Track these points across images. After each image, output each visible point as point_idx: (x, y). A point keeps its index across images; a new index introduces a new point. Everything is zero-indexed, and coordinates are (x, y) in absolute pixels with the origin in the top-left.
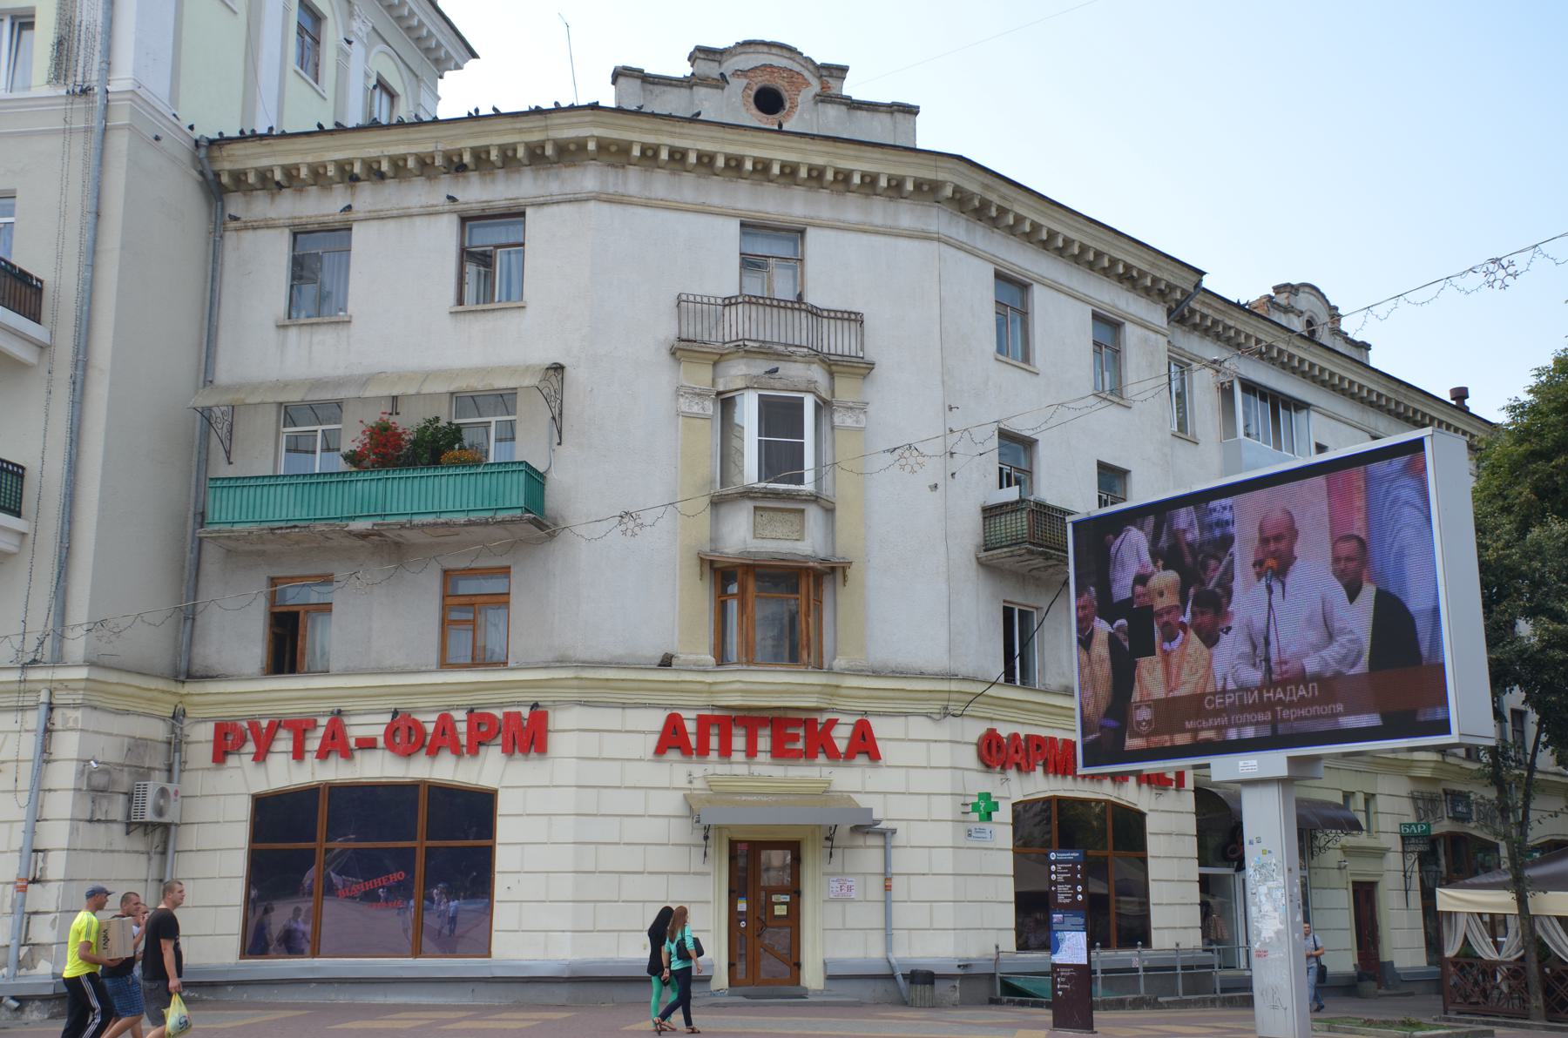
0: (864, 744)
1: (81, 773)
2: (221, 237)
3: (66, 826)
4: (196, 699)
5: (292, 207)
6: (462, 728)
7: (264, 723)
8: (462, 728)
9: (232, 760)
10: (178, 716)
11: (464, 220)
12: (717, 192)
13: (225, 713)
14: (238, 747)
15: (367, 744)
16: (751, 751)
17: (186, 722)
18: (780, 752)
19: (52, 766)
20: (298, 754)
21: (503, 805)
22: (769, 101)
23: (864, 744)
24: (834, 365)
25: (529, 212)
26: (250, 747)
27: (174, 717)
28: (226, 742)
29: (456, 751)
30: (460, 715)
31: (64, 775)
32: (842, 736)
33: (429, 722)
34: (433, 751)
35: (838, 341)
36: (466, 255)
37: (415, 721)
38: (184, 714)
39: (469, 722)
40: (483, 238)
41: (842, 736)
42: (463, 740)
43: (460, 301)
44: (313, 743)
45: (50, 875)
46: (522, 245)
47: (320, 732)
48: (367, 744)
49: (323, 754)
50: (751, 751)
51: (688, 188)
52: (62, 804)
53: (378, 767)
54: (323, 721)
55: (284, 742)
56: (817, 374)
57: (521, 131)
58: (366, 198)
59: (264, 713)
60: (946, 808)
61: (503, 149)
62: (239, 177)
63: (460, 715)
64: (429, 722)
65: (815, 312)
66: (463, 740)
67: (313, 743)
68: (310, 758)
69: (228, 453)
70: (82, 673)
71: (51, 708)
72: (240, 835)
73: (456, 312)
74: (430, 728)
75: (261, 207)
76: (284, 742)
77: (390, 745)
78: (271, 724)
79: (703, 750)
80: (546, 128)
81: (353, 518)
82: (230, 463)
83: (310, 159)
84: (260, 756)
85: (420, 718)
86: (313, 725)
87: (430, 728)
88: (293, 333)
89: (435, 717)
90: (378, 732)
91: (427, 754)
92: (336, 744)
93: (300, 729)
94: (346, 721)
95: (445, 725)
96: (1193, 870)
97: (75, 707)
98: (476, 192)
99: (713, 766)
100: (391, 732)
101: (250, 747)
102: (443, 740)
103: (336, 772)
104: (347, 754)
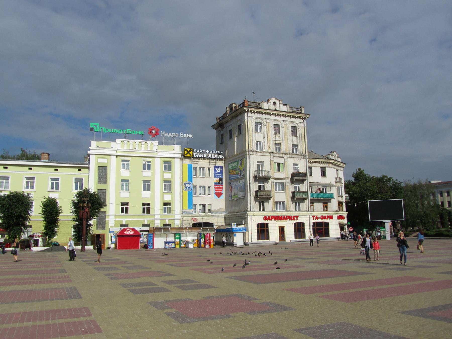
21: (330, 224)
33: (324, 216)
49: (316, 219)
53: (320, 220)
54: (315, 216)
68: (315, 219)
86: (315, 216)
90: (320, 217)
100: (321, 217)
104: (318, 219)
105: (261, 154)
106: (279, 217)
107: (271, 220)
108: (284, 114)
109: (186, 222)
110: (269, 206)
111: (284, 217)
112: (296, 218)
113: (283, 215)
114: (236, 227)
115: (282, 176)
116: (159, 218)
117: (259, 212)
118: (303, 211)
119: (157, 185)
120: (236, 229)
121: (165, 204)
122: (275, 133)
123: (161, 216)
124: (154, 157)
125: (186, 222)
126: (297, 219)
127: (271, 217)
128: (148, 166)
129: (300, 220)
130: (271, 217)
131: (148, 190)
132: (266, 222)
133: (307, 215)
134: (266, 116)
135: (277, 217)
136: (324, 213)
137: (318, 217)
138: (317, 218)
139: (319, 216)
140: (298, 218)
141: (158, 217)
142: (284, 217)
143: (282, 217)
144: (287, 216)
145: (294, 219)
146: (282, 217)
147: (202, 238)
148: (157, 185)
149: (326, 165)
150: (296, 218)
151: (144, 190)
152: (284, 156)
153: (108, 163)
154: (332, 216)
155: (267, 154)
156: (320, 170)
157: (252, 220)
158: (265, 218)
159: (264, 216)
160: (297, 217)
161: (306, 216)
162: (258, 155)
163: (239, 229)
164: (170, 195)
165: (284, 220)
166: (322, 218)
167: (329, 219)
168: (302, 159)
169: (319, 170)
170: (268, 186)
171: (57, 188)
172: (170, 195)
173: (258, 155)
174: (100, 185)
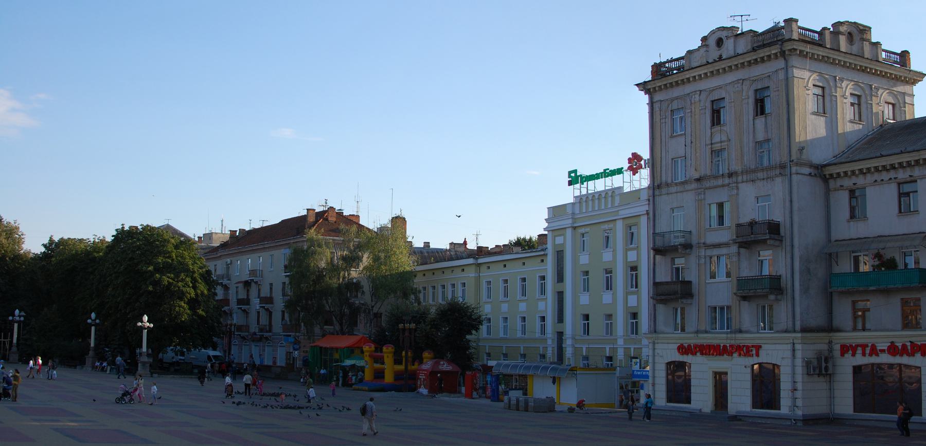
1: (803, 362)
2: (829, 194)
3: (801, 376)
4: (834, 338)
5: (848, 183)
6: (909, 348)
7: (854, 345)
8: (909, 348)
9: (846, 355)
10: (830, 342)
11: (899, 184)
14: (847, 351)
17: (833, 344)
19: (796, 360)
20: (864, 354)
25: (918, 181)
26: (850, 352)
27: (829, 343)
28: (844, 349)
29: (908, 355)
30: (908, 344)
31: (799, 362)
33: (899, 345)
34: (901, 355)
36: (901, 195)
37: (896, 346)
38: (832, 342)
39: (911, 346)
40: (906, 188)
42: (910, 351)
43: (900, 212)
44: (868, 351)
45: (798, 389)
46: (917, 191)
47: (869, 348)
49: (870, 355)
52: (799, 370)
53: (885, 358)
54: (870, 345)
55: (859, 350)
57: (911, 157)
58: (870, 178)
59: (854, 342)
61: (908, 162)
62: (831, 175)
63: (908, 344)
64: (899, 345)
66: (910, 351)
67: (868, 351)
69: (837, 262)
70: (799, 335)
71: (794, 344)
72: (850, 377)
73: (899, 216)
74: (900, 347)
75: (839, 182)
76: (859, 350)
77: (889, 353)
78: (855, 345)
80: (919, 155)
81: (871, 286)
82: (838, 265)
83: (850, 169)
84: (854, 355)
85: (897, 344)
86: (867, 346)
87: (900, 347)
88: (852, 223)
89: (901, 344)
90: (886, 348)
91: (900, 356)
92: (874, 351)
93: (864, 347)
94: (876, 345)
95: (904, 346)
97: (799, 344)
98: (902, 175)
101: (850, 352)
102: (904, 351)
103: (874, 360)
104: (877, 355)
105: (679, 188)
107: (694, 354)
108: (702, 71)
110: (695, 316)
113: (721, 341)
114: (639, 369)
116: (623, 344)
117: (673, 335)
118: (778, 332)
120: (639, 373)
122: (713, 124)
124: (615, 220)
126: (757, 355)
129: (764, 357)
133: (788, 341)
136: (906, 336)
137: (879, 348)
138: (874, 351)
140: (761, 352)
141: (620, 342)
144: (696, 346)
147: (500, 384)
149: (860, 181)
152: (727, 181)
155: (688, 187)
156: (867, 196)
157: (656, 354)
158: (684, 350)
159: (679, 345)
160: (758, 348)
161: (785, 347)
162: (672, 193)
163: (644, 373)
164: (636, 296)
165: (725, 356)
166: (893, 350)
167: (918, 355)
168: (779, 180)
169: (891, 191)
172: (636, 296)
173: (672, 193)
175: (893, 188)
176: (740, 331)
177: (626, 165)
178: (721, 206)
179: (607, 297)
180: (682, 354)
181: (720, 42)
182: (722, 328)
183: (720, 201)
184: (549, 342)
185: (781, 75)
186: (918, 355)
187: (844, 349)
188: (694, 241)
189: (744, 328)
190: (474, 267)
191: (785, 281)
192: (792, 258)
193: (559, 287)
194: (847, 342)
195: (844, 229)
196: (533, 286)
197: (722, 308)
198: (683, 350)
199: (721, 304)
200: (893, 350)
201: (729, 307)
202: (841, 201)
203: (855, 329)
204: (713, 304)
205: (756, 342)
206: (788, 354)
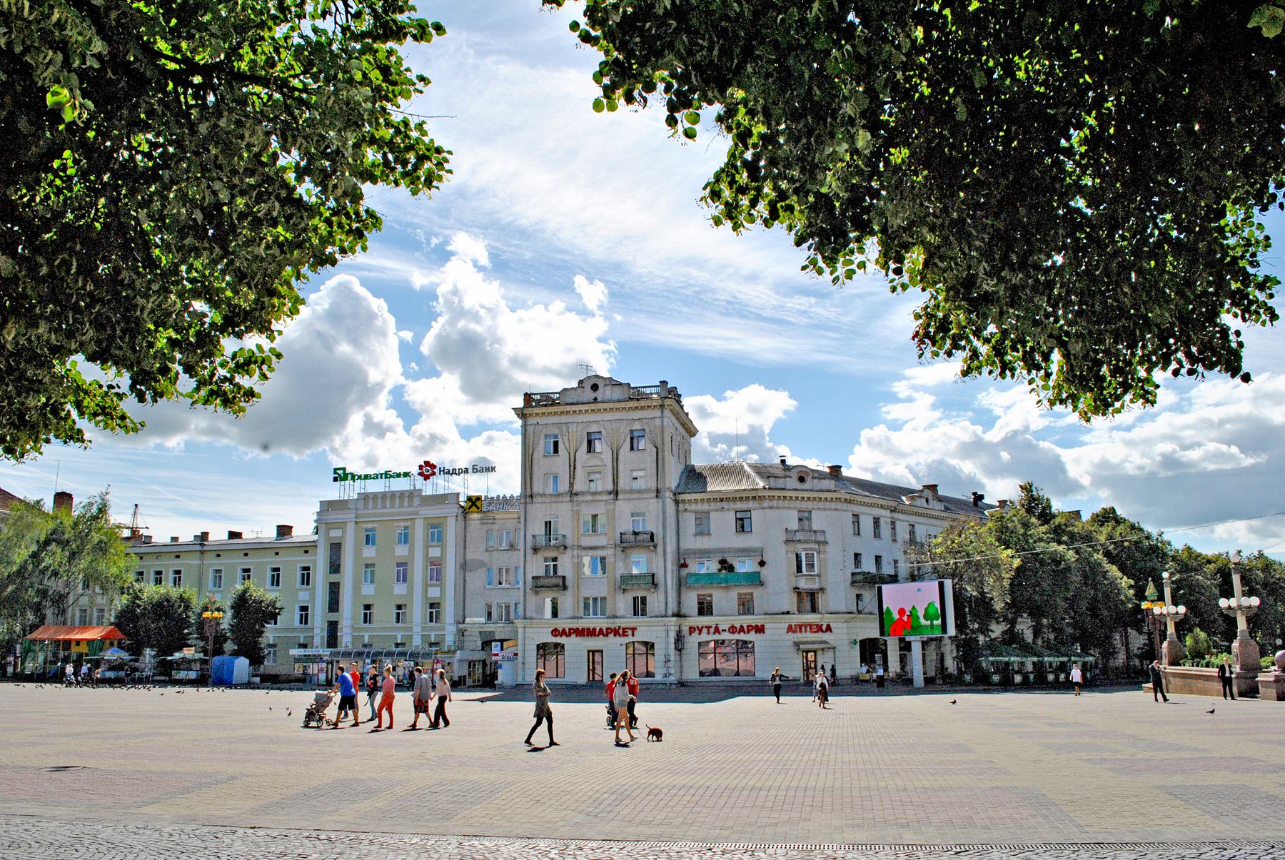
0: (829, 629)
12: (792, 504)
13: (691, 624)
15: (724, 630)
16: (806, 631)
18: (811, 631)
20: (709, 633)
22: (802, 479)
23: (829, 629)
24: (819, 543)
28: (692, 630)
32: (824, 628)
33: (738, 626)
35: (820, 538)
41: (824, 628)
48: (724, 630)
50: (806, 631)
51: (786, 504)
55: (705, 631)
56: (817, 546)
60: (846, 642)
62: (684, 501)
64: (738, 626)
65: (815, 532)
67: (712, 630)
75: (687, 506)
79: (795, 632)
92: (717, 630)
93: (709, 627)
96: (898, 653)
98: (739, 506)
99: (798, 634)
101: (697, 632)
102: (742, 630)
106: (589, 629)
109: (471, 638)
110: (568, 602)
111: (601, 630)
112: (630, 632)
115: (602, 541)
119: (418, 572)
121: (432, 606)
123: (423, 629)
125: (471, 638)
127: (570, 629)
128: (406, 538)
130: (570, 629)
131: (404, 581)
132: (559, 640)
134: (564, 419)
135: (583, 629)
139: (724, 626)
142: (601, 630)
143: (594, 629)
145: (624, 634)
146: (594, 629)
148: (418, 572)
150: (630, 632)
151: (398, 580)
153: (341, 538)
154: (763, 626)
160: (633, 629)
161: (660, 628)
166: (732, 629)
167: (752, 633)
170: (537, 567)
171: (278, 584)
174: (333, 575)
175: (731, 517)
176: (615, 617)
177: (416, 470)
178: (595, 517)
179: (400, 589)
180: (556, 636)
181: (595, 387)
182: (595, 613)
183: (595, 513)
184: (317, 631)
185: (658, 422)
186: (752, 633)
187: (692, 630)
188: (569, 542)
189: (619, 614)
190: (198, 553)
191: (660, 578)
192: (665, 561)
193: (334, 578)
194: (694, 625)
195: (691, 542)
196: (291, 575)
197: (595, 599)
198: (555, 632)
199: (595, 596)
200: (732, 629)
201: (604, 599)
202: (689, 521)
203: (800, 611)
204: (587, 596)
205: (632, 625)
206: (664, 634)
